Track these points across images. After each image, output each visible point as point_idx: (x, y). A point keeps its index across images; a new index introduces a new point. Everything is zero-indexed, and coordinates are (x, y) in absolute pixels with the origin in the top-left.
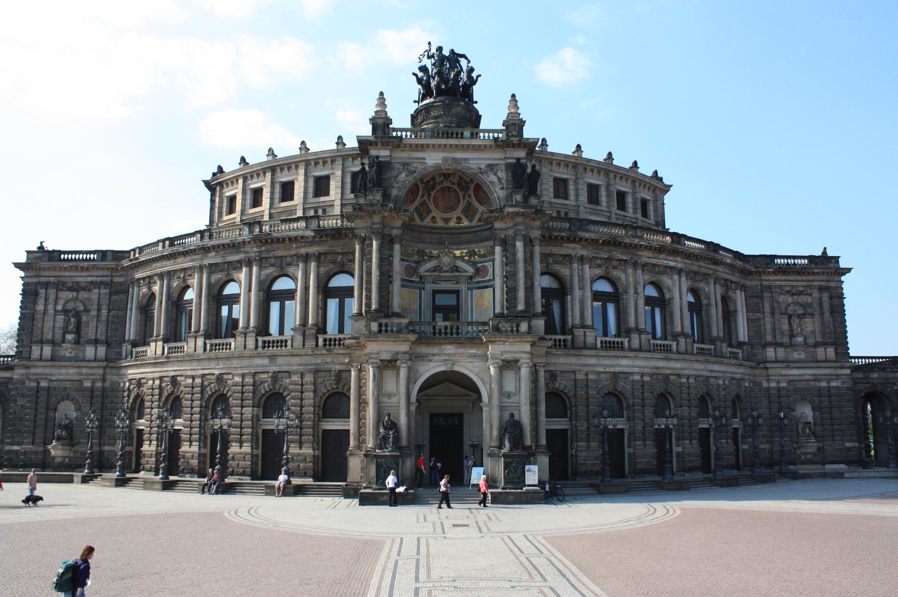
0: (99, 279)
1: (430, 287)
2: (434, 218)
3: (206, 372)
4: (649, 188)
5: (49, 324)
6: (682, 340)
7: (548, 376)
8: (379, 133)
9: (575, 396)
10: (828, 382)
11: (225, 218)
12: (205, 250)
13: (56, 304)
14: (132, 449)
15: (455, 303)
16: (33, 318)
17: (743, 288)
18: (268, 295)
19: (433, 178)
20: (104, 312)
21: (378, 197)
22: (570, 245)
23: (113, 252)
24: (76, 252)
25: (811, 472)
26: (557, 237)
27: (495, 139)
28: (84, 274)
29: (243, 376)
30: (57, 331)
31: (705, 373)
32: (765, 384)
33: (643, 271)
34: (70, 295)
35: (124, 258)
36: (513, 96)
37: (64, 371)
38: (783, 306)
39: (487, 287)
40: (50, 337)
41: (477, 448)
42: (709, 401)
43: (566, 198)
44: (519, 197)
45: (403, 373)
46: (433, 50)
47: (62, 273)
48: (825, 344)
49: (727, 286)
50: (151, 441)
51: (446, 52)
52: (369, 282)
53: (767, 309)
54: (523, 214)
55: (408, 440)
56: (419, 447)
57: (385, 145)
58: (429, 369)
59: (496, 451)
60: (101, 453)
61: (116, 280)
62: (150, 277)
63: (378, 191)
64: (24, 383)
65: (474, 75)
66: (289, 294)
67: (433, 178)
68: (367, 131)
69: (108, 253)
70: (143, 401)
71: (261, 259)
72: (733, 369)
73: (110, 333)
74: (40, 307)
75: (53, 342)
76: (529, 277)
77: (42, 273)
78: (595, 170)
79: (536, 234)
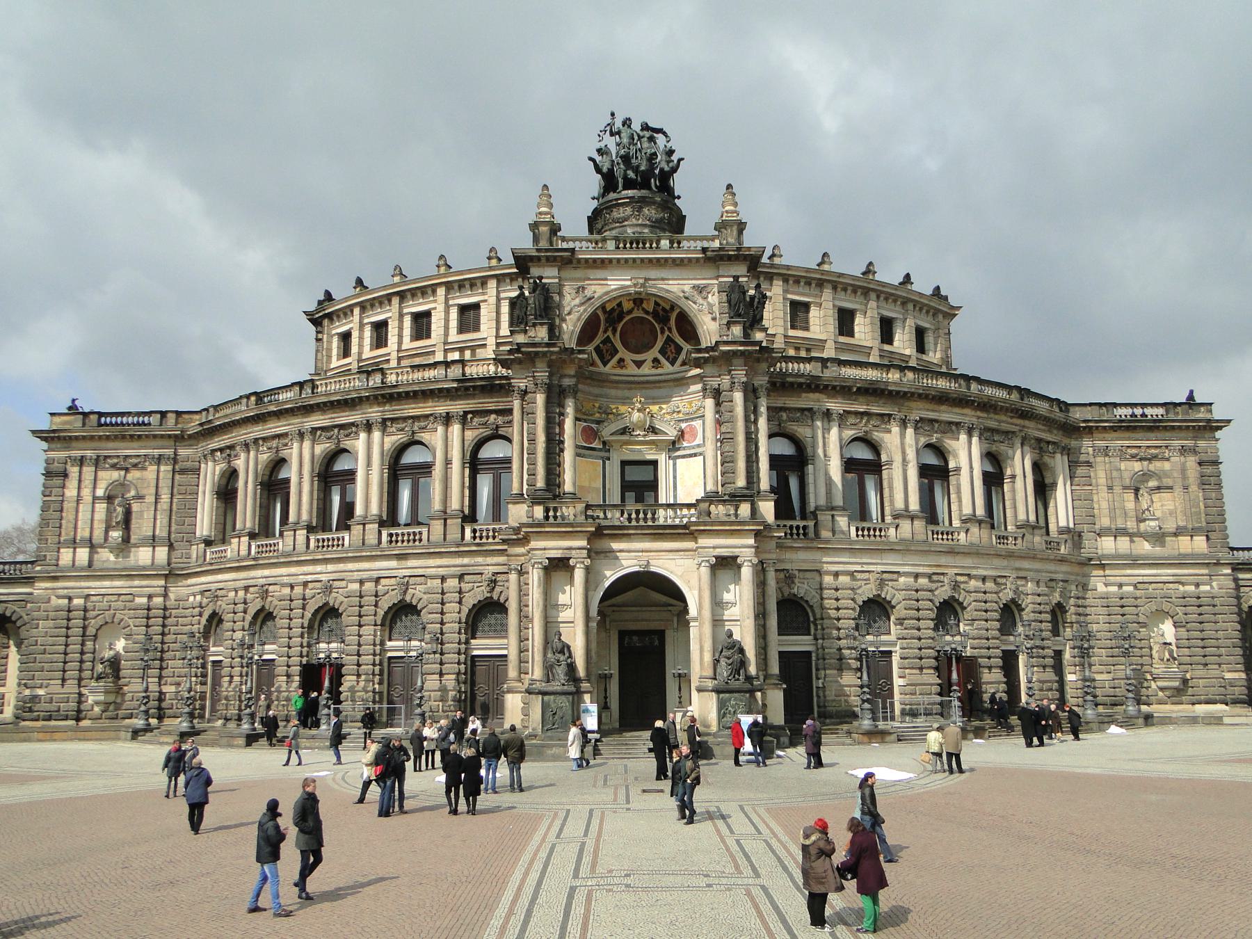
0: (156, 452)
1: (616, 458)
2: (621, 360)
3: (309, 578)
4: (928, 312)
5: (84, 514)
6: (975, 530)
7: (782, 575)
8: (543, 244)
9: (822, 607)
10: (1197, 585)
11: (335, 363)
12: (308, 410)
13: (95, 487)
14: (208, 688)
15: (652, 478)
16: (61, 511)
17: (1066, 450)
18: (396, 470)
19: (620, 305)
20: (165, 498)
21: (541, 333)
22: (811, 395)
23: (179, 414)
24: (122, 414)
25: (1174, 715)
26: (792, 384)
27: (704, 250)
28: (135, 444)
29: (362, 582)
30: (96, 525)
32: (1101, 588)
33: (916, 429)
34: (116, 475)
35: (191, 421)
36: (729, 187)
37: (107, 583)
38: (1126, 475)
39: (695, 455)
40: (87, 534)
41: (684, 678)
42: (1016, 612)
43: (807, 329)
44: (737, 331)
45: (579, 574)
46: (618, 124)
47: (103, 444)
48: (1193, 533)
49: (1041, 448)
50: (232, 677)
51: (636, 126)
52: (532, 453)
53: (1102, 481)
54: (742, 353)
55: (588, 669)
56: (605, 678)
57: (551, 261)
59: (710, 684)
62: (231, 447)
63: (542, 324)
64: (49, 601)
65: (675, 158)
66: (426, 469)
67: (620, 305)
68: (526, 243)
69: (169, 415)
70: (221, 621)
71: (385, 420)
72: (1051, 567)
73: (173, 529)
74: (71, 492)
76: (751, 439)
77: (74, 444)
78: (850, 288)
79: (761, 381)
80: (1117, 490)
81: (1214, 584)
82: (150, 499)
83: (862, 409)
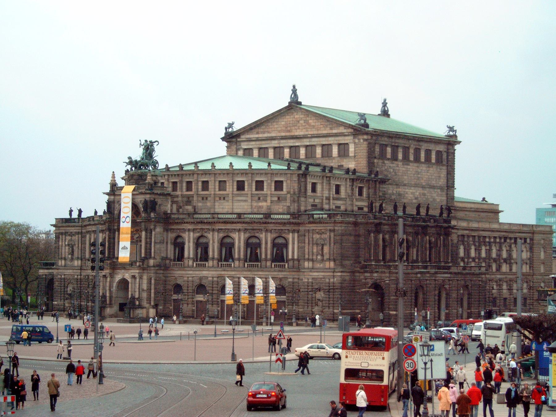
0: (77, 231)
5: (63, 251)
6: (237, 263)
22: (185, 225)
28: (73, 228)
31: (251, 276)
37: (68, 271)
43: (225, 190)
45: (108, 279)
48: (329, 260)
53: (307, 241)
58: (118, 277)
60: (81, 305)
61: (83, 231)
74: (60, 243)
75: (65, 259)
79: (152, 227)
80: (311, 245)
81: (335, 279)
82: (77, 246)
83: (200, 227)
